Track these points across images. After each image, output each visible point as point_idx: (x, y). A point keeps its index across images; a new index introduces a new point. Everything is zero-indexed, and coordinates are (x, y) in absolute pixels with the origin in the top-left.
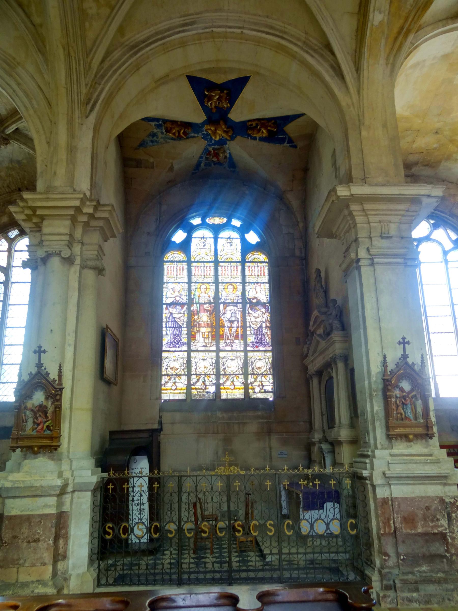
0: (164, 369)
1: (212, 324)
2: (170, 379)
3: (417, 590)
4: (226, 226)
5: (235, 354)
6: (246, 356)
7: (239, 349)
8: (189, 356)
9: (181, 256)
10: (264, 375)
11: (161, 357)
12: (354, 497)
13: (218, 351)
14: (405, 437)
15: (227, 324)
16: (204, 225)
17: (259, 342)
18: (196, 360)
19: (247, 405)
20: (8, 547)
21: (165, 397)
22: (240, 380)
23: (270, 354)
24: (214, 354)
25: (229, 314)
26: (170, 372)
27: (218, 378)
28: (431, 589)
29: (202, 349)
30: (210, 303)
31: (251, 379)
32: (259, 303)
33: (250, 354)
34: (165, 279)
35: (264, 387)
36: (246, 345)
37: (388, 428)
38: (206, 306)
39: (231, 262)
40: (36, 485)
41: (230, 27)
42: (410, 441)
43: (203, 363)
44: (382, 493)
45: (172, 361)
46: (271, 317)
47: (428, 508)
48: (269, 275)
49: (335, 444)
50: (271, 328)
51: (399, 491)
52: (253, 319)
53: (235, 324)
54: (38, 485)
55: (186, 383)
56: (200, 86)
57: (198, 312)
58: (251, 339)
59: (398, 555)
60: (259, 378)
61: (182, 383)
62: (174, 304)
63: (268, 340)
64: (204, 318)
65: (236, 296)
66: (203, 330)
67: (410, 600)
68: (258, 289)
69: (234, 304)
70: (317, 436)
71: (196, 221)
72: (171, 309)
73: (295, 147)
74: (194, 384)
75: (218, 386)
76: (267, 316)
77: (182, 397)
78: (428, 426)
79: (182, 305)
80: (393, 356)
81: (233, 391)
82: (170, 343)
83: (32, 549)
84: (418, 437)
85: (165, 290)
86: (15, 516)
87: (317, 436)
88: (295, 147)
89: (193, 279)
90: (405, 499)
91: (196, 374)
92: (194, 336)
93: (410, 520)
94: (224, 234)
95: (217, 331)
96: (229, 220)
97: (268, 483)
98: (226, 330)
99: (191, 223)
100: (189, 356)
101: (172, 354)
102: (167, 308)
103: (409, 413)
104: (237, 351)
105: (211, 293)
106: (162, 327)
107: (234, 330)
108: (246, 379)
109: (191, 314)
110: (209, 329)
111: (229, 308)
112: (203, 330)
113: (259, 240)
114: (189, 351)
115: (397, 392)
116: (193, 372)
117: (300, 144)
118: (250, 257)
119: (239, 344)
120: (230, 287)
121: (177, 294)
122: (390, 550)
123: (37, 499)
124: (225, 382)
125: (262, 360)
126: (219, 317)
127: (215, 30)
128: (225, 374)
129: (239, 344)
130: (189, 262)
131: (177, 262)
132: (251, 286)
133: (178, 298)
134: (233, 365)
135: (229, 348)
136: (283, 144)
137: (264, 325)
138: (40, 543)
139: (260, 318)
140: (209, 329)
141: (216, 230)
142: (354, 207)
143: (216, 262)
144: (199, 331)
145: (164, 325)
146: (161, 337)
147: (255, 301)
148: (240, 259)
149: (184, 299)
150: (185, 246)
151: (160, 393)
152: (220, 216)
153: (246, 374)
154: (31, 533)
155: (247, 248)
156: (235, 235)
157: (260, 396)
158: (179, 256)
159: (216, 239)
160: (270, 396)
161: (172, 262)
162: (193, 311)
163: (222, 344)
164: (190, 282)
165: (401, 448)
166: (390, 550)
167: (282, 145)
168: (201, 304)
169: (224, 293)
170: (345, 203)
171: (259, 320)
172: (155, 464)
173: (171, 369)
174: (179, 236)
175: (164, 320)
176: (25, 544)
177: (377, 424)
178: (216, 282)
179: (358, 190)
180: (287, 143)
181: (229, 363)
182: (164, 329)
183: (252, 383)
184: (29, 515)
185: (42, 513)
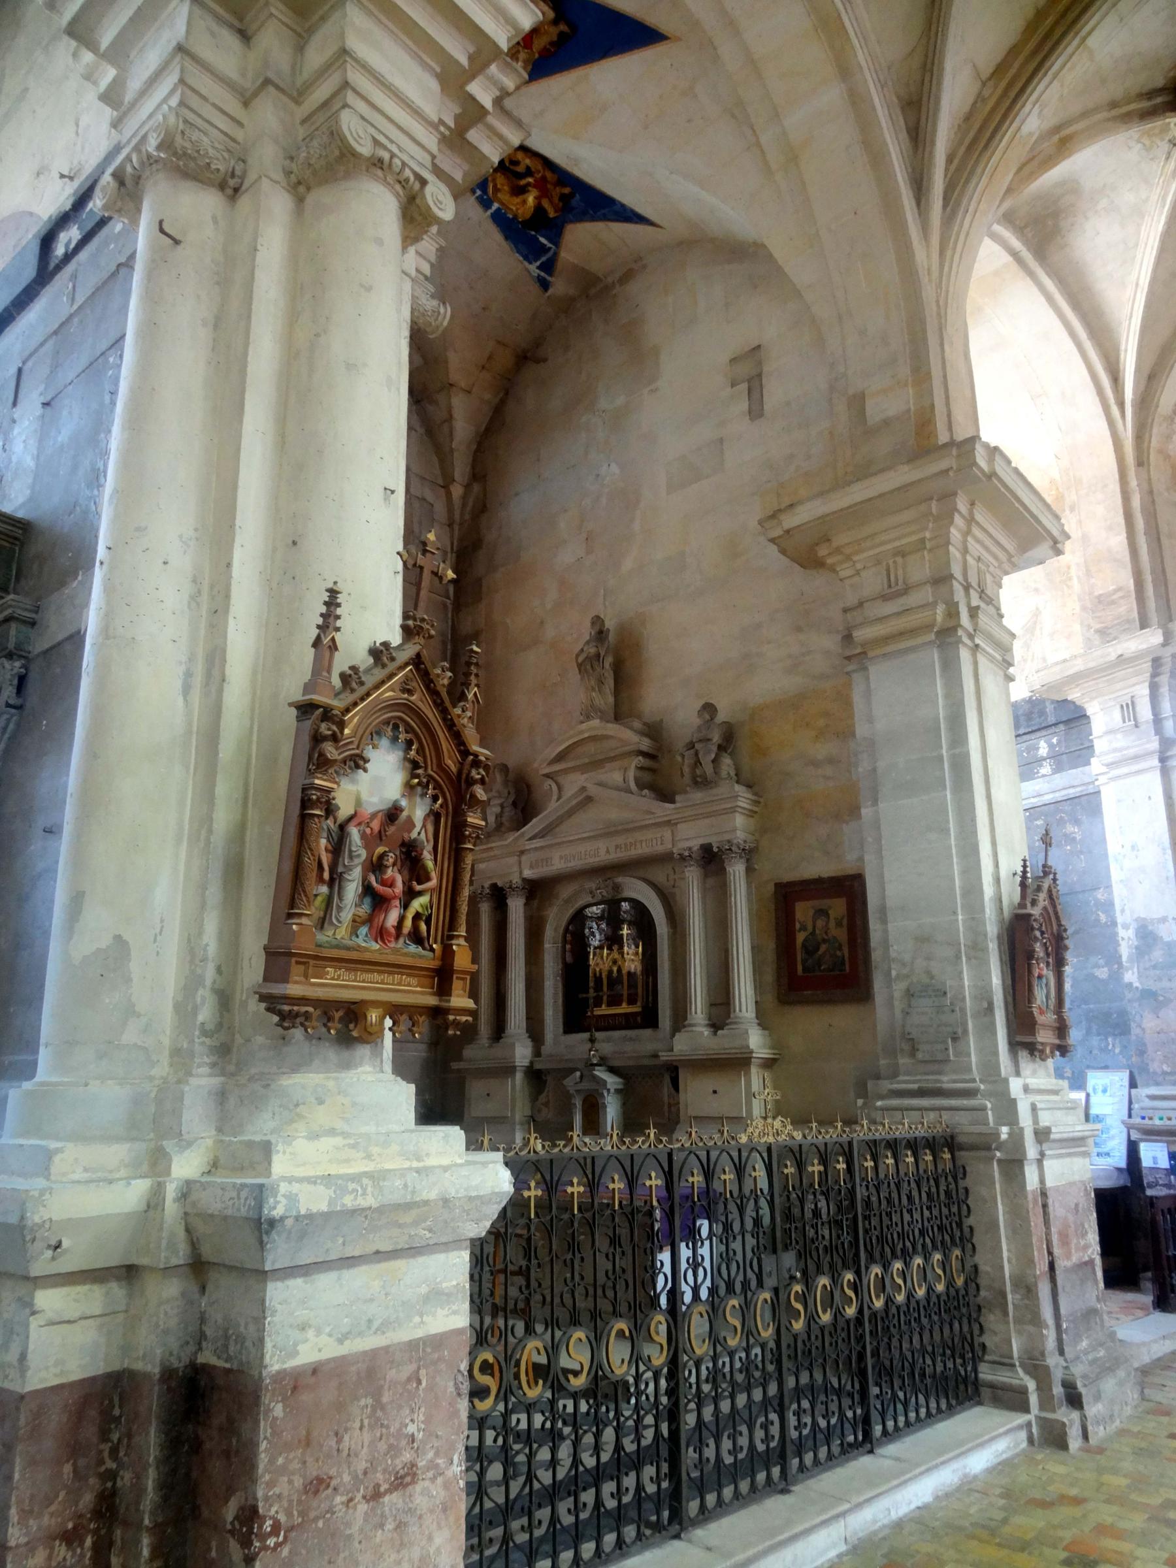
20: (285, 1551)
40: (425, 1195)
54: (433, 1195)
73: (544, 285)
83: (390, 1526)
86: (315, 1370)
88: (544, 285)
117: (560, 286)
123: (399, 1264)
136: (530, 263)
138: (418, 1488)
154: (382, 1446)
167: (526, 264)
176: (363, 1507)
180: (538, 268)
184: (374, 1354)
185: (419, 1333)
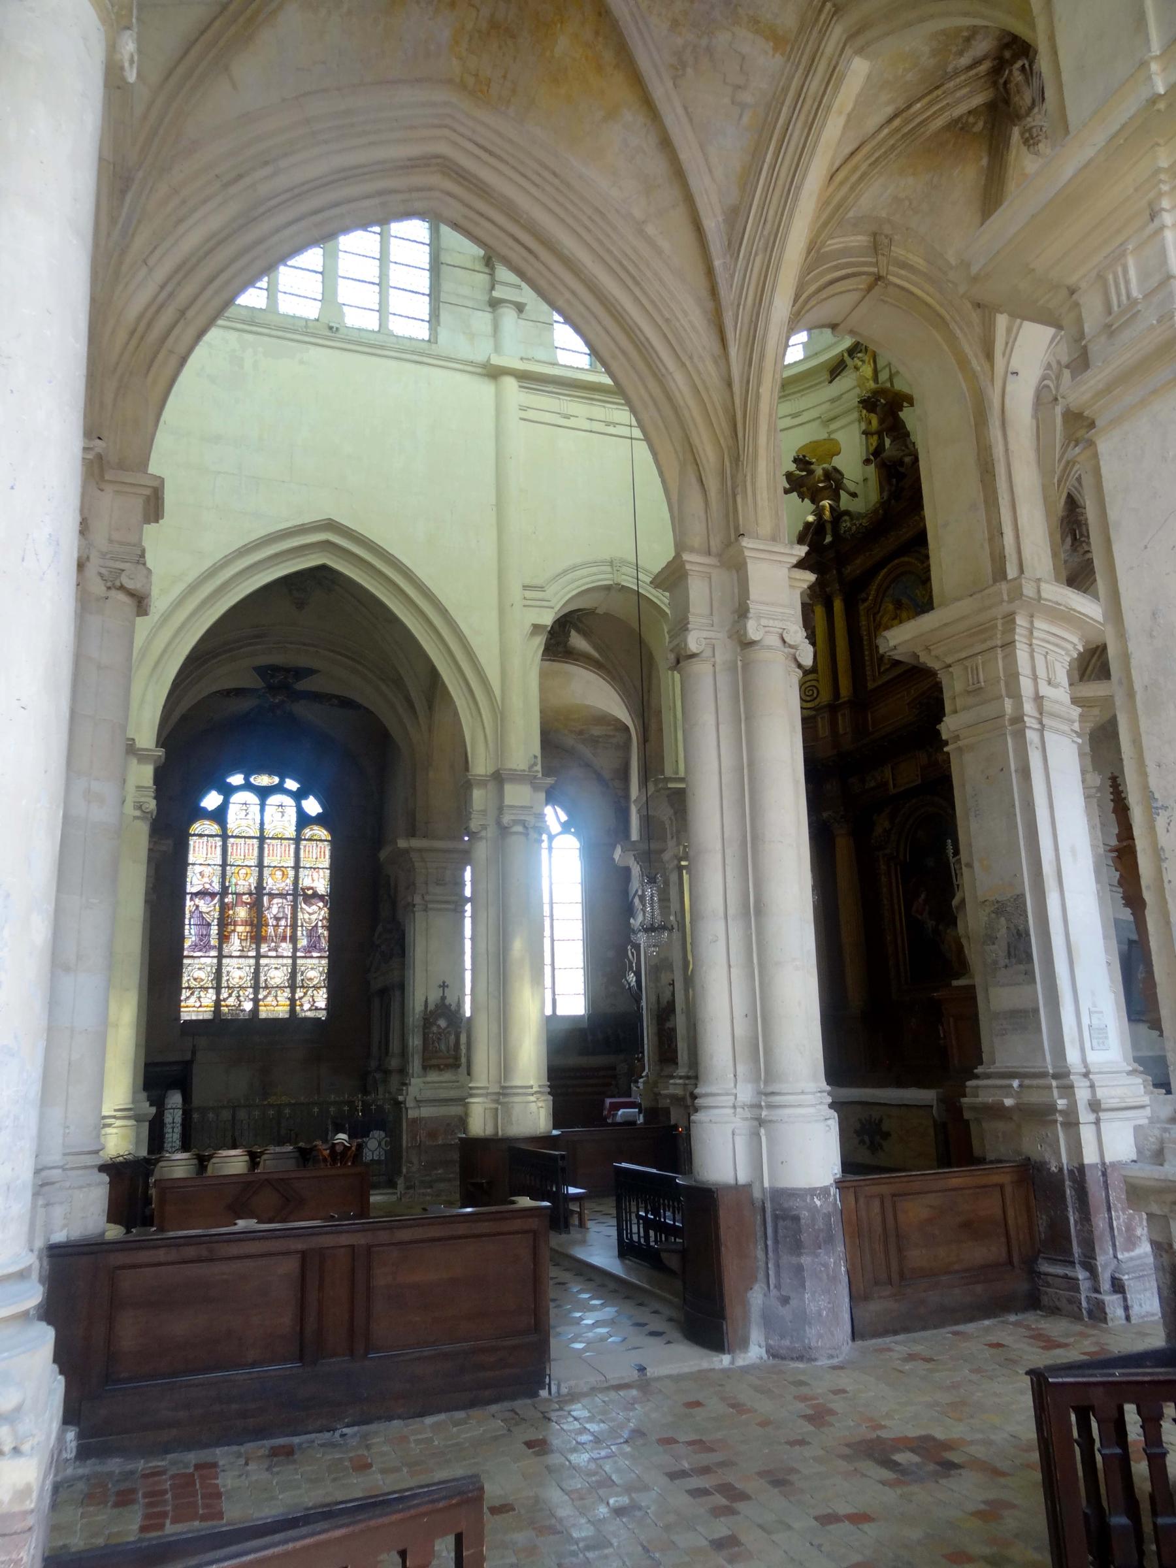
0: (185, 979)
1: (252, 922)
2: (192, 994)
3: (431, 1187)
4: (279, 789)
5: (280, 961)
6: (294, 965)
7: (285, 954)
8: (220, 964)
9: (214, 828)
10: (316, 988)
11: (181, 965)
12: (387, 1118)
13: (258, 957)
14: (439, 1068)
15: (272, 922)
16: (248, 786)
17: (312, 947)
18: (229, 969)
19: (293, 1023)
21: (185, 1016)
22: (286, 995)
23: (324, 962)
24: (252, 961)
25: (274, 908)
26: (193, 984)
27: (256, 993)
28: (442, 1186)
29: (238, 954)
30: (250, 894)
31: (299, 994)
32: (315, 895)
33: (299, 961)
34: (191, 859)
35: (315, 1002)
36: (295, 950)
37: (424, 1060)
38: (245, 898)
39: (281, 839)
41: (304, 644)
42: (441, 1070)
43: (238, 972)
44: (412, 1114)
45: (197, 969)
46: (330, 914)
47: (448, 1125)
48: (331, 857)
49: (387, 1072)
50: (329, 928)
51: (426, 1112)
52: (306, 916)
53: (283, 923)
55: (214, 998)
56: (265, 672)
57: (233, 906)
58: (303, 942)
59: (420, 1162)
60: (310, 992)
61: (209, 998)
62: (202, 894)
63: (324, 944)
64: (242, 913)
65: (286, 885)
66: (240, 929)
67: (424, 1195)
68: (315, 875)
69: (282, 895)
70: (373, 1064)
71: (237, 779)
72: (197, 901)
74: (225, 1000)
75: (256, 1001)
76: (324, 912)
77: (208, 1016)
78: (457, 1058)
79: (213, 895)
80: (434, 996)
81: (275, 1007)
82: (195, 946)
84: (448, 1067)
85: (189, 874)
87: (373, 1064)
89: (230, 860)
90: (431, 1118)
91: (228, 987)
92: (228, 938)
93: (432, 1135)
94: (274, 799)
95: (259, 931)
96: (282, 782)
97: (316, 1110)
98: (271, 930)
99: (230, 784)
100: (220, 964)
101: (196, 961)
102: (191, 899)
103: (443, 1047)
104: (282, 957)
105: (253, 881)
106: (184, 925)
107: (281, 930)
108: (293, 992)
109: (224, 907)
110: (248, 929)
111: (275, 901)
112: (240, 929)
113: (320, 810)
114: (220, 957)
115: (435, 1029)
116: (224, 984)
118: (307, 832)
119: (286, 948)
120: (279, 873)
121: (206, 880)
122: (415, 1161)
124: (265, 997)
125: (315, 969)
126: (262, 913)
127: (289, 646)
128: (266, 987)
129: (286, 948)
130: (225, 836)
131: (208, 836)
132: (307, 872)
133: (207, 886)
134: (277, 975)
135: (273, 954)
137: (320, 924)
139: (315, 914)
140: (248, 929)
141: (263, 793)
142: (415, 856)
143: (262, 839)
144: (234, 931)
145: (187, 922)
146: (182, 938)
147: (310, 892)
148: (293, 834)
149: (216, 887)
150: (219, 815)
151: (179, 1012)
152: (271, 773)
153: (293, 987)
155: (304, 820)
156: (289, 801)
157: (309, 1014)
158: (211, 827)
159: (263, 806)
160: (322, 1015)
161: (201, 836)
162: (227, 904)
163: (264, 948)
164: (224, 865)
165: (433, 1077)
166: (415, 1161)
168: (238, 895)
169: (270, 881)
170: (407, 851)
171: (314, 917)
172: (186, 1099)
173: (195, 979)
174: (211, 801)
175: (187, 916)
177: (416, 1056)
178: (260, 865)
179: (415, 843)
181: (273, 973)
182: (187, 927)
183: (301, 998)
